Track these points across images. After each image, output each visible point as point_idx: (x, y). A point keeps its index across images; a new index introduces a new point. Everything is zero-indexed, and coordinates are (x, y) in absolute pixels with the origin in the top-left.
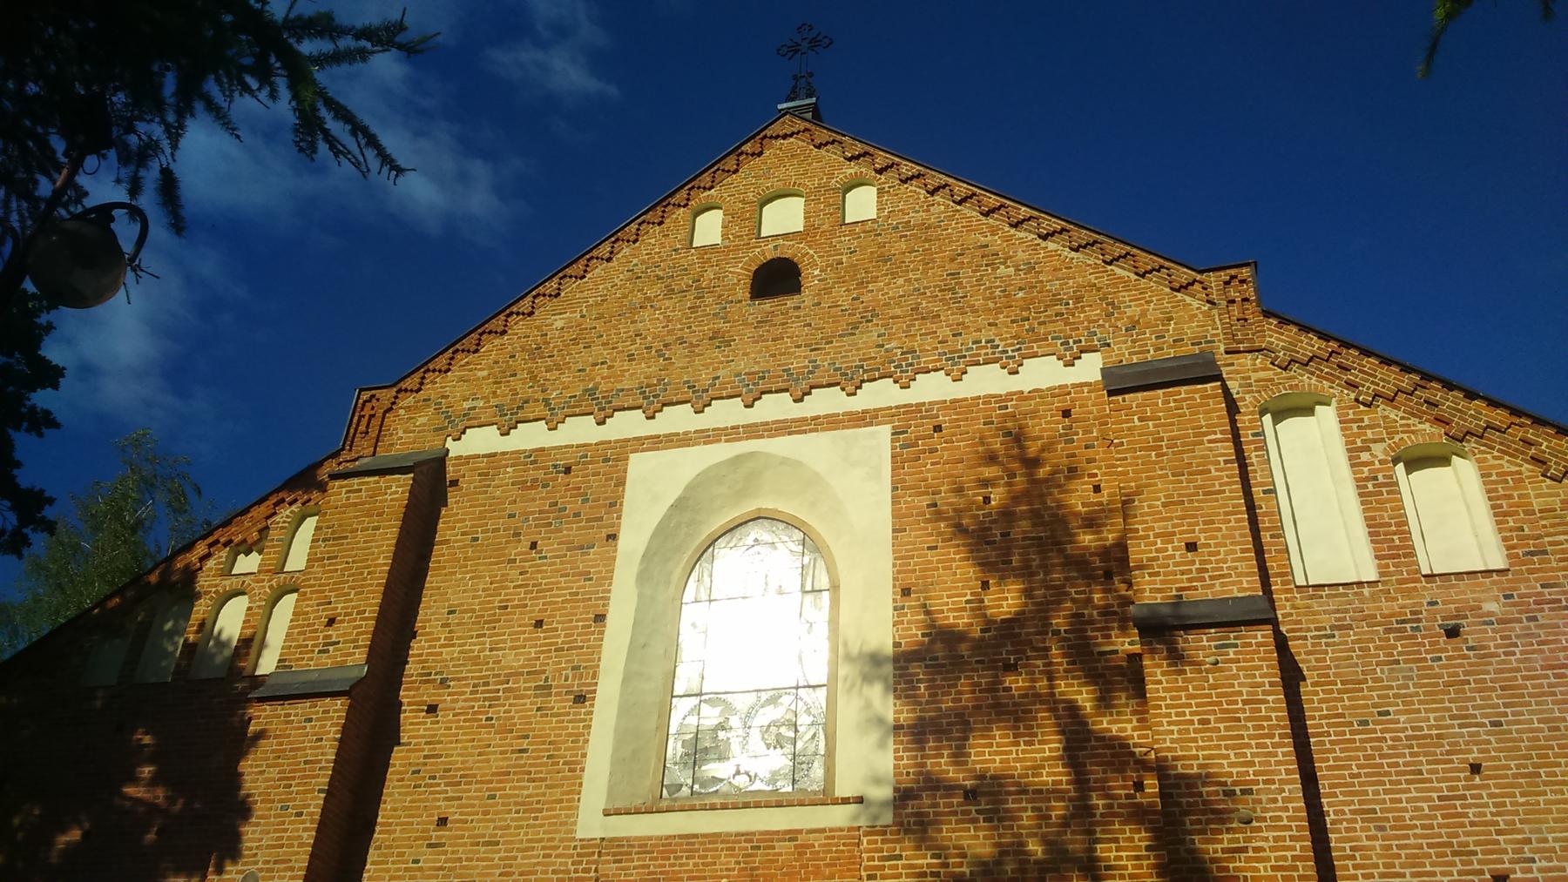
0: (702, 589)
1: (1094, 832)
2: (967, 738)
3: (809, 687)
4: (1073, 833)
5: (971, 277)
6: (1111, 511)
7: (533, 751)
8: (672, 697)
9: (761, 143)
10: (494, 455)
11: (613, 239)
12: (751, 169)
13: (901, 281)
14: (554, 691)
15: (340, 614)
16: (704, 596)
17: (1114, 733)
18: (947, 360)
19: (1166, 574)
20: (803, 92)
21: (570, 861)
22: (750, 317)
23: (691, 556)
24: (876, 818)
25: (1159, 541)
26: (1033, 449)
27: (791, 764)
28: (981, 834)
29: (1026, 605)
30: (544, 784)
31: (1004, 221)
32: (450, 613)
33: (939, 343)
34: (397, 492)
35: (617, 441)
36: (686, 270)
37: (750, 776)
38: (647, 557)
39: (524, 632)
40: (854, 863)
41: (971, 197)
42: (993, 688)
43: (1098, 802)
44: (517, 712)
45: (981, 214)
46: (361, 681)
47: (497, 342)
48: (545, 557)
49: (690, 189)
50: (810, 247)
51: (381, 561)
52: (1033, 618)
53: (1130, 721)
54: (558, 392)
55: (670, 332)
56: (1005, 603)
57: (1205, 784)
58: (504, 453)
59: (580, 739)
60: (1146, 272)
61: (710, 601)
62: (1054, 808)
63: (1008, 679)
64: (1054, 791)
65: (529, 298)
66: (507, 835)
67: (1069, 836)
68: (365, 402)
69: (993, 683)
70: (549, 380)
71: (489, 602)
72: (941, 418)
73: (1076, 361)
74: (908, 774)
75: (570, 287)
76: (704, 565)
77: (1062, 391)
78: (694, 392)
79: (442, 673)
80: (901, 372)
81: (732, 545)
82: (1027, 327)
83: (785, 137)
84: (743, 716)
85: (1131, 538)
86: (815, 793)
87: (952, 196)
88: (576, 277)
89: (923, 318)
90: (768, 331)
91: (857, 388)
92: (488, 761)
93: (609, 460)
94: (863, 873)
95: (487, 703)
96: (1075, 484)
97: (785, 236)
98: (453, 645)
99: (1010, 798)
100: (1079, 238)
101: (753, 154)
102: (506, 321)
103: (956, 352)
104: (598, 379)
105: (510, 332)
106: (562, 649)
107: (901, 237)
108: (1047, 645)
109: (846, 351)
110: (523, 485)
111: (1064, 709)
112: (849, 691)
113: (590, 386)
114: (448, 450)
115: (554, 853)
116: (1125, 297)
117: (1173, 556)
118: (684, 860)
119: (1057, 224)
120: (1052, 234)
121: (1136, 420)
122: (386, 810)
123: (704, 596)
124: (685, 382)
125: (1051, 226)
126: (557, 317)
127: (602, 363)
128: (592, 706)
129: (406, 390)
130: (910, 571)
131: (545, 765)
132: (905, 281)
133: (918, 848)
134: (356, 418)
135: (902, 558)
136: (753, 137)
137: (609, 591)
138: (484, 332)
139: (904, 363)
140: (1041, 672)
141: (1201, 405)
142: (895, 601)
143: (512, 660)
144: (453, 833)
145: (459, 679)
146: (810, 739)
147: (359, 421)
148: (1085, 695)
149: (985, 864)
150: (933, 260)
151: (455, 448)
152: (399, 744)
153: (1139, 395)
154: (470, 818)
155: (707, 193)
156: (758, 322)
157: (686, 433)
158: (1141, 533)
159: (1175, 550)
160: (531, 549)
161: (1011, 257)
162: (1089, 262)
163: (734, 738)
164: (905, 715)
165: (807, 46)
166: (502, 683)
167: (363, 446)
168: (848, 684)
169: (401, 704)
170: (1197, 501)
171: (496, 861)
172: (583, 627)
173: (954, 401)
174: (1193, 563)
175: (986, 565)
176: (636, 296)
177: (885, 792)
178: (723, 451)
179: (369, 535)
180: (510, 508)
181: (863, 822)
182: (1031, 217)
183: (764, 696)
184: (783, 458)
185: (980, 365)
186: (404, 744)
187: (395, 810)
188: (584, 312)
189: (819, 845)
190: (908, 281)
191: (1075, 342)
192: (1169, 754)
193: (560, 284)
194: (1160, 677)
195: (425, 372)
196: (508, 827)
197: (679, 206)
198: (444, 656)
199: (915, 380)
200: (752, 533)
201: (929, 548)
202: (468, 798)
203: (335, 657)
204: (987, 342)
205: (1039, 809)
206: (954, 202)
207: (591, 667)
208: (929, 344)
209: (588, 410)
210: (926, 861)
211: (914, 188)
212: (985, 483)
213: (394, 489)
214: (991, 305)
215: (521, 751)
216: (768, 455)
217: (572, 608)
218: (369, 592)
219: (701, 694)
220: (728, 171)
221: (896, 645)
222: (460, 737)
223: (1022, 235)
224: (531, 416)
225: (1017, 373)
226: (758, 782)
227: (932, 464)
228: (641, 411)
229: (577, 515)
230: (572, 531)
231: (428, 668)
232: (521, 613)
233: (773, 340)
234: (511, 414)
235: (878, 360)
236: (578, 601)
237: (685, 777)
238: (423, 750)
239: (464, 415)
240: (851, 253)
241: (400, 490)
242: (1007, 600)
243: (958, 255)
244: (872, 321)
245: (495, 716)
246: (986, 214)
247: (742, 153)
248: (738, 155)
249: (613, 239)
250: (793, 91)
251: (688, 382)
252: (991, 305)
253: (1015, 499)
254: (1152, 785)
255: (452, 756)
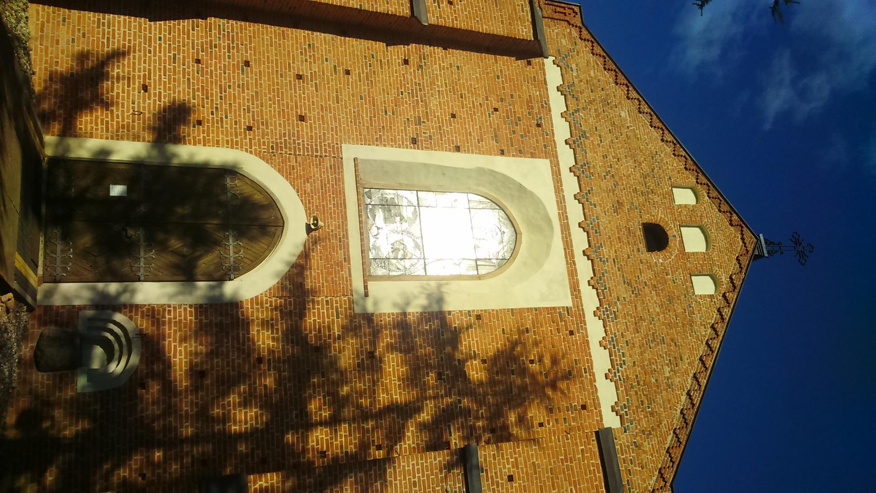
0: (476, 204)
1: (354, 423)
2: (401, 352)
3: (425, 265)
4: (353, 411)
5: (662, 351)
6: (529, 432)
7: (386, 118)
8: (417, 191)
9: (738, 225)
10: (546, 83)
11: (675, 142)
12: (722, 220)
13: (658, 310)
14: (418, 127)
15: (455, 7)
16: (472, 205)
17: (407, 434)
18: (612, 338)
19: (495, 464)
20: (770, 248)
21: (330, 142)
22: (632, 224)
23: (493, 197)
24: (357, 304)
25: (513, 460)
26: (563, 385)
27: (384, 257)
28: (351, 361)
29: (474, 384)
30: (369, 125)
31: (697, 370)
32: (458, 67)
33: (622, 333)
34: (523, 32)
35: (556, 151)
36: (659, 185)
37: (377, 235)
38: (493, 173)
39: (449, 108)
40: (334, 293)
41: (711, 350)
42: (429, 366)
43: (370, 424)
44: (406, 107)
45: (701, 356)
46: (419, 22)
47: (611, 80)
48: (490, 117)
49: (707, 184)
50: (676, 256)
51: (484, 27)
52: (467, 389)
53: (413, 443)
54: (583, 117)
55: (621, 178)
56: (475, 373)
57: (381, 484)
58: (547, 89)
59: (394, 142)
60: (670, 454)
61: (469, 209)
62: (366, 400)
63: (433, 375)
64: (375, 401)
65: (637, 96)
66: (342, 107)
67: (352, 409)
68: (573, 9)
69: (431, 366)
70: (590, 111)
71: (464, 87)
72: (578, 335)
73: (615, 413)
74: (381, 321)
75: (645, 119)
76: (489, 204)
77: (597, 405)
78: (586, 193)
79: (425, 65)
80: (604, 311)
81: (501, 219)
82: (634, 384)
83: (743, 239)
84: (408, 230)
85: (514, 444)
86: (370, 271)
87: (711, 339)
88: (651, 122)
89: (636, 323)
90: (624, 234)
91: (593, 286)
92: (380, 94)
93: (545, 148)
94: (329, 298)
95: (410, 91)
96: (543, 411)
97: (682, 242)
98: (440, 71)
99: (370, 377)
100: (689, 414)
101: (731, 220)
102: (623, 84)
103: (617, 343)
104: (592, 139)
105: (617, 87)
106: (440, 130)
107: (685, 310)
108: (453, 396)
109: (614, 279)
110: (529, 102)
111: (419, 406)
112: (423, 287)
113: (587, 135)
114: (547, 58)
115: (334, 133)
116: (655, 441)
117: (505, 467)
118: (332, 202)
119: (697, 401)
120: (690, 398)
121: (582, 447)
122: (352, 42)
123: (472, 205)
124: (592, 188)
125: (695, 398)
126: (627, 113)
127: (601, 140)
128: (411, 148)
129: (581, 32)
130: (490, 318)
131: (379, 125)
132: (658, 313)
133: (343, 327)
134: (563, 5)
135: (497, 314)
136: (741, 220)
137: (472, 153)
138: (616, 72)
139: (608, 313)
140: (437, 393)
141: (592, 485)
142: (474, 311)
143: (433, 103)
144: (342, 79)
145: (422, 75)
146: (398, 267)
147: (562, 7)
148: (426, 417)
149: (336, 363)
150: (671, 328)
151: (548, 62)
152: (387, 46)
153: (597, 449)
154: (350, 87)
155: (706, 194)
156: (629, 228)
157: (562, 190)
158: (517, 450)
159: (509, 469)
160: (494, 109)
161: (675, 374)
162: (674, 420)
163: (397, 225)
164: (412, 318)
165: (800, 250)
166: (421, 98)
167: (548, 10)
168: (427, 287)
169: (408, 45)
170: (537, 482)
171: (328, 103)
172: (453, 140)
173: (588, 342)
174: (502, 479)
175: (495, 359)
176: (641, 157)
177: (370, 308)
178: (553, 211)
179: (498, 19)
180: (516, 95)
181: (355, 296)
182: (700, 386)
183: (419, 241)
184: (551, 246)
185: (610, 357)
186: (387, 49)
187: (353, 46)
188: (630, 128)
189: (343, 274)
190: (658, 314)
191: (626, 412)
192: (397, 465)
193: (647, 113)
194: (438, 459)
195: (591, 41)
196: (346, 108)
197: (697, 179)
198: (435, 66)
199: (599, 319)
200: (508, 230)
201: (503, 329)
202: (360, 85)
203: (432, 7)
204: (624, 361)
205: (365, 393)
206: (708, 340)
207: (431, 146)
208: (620, 327)
209: (574, 135)
210: (336, 331)
211: (715, 316)
212: (541, 360)
213: (524, 30)
214: (646, 363)
215: (386, 112)
216: (552, 237)
217: (463, 133)
218: (467, 22)
219: (419, 206)
220: (720, 207)
221: (450, 312)
222: (392, 78)
223: (690, 381)
224: (569, 103)
225: (606, 379)
226: (374, 239)
227: (551, 330)
228: (574, 164)
229: (514, 132)
230: (505, 131)
231: (428, 58)
232: (459, 106)
233: (619, 237)
234: (569, 91)
235: (610, 298)
236: (467, 136)
237: (375, 200)
238: (384, 59)
239: (568, 65)
240: (673, 280)
241: (524, 34)
242: (476, 372)
243: (675, 344)
244: (633, 294)
245: (404, 96)
246: (701, 359)
247: (731, 214)
248: (730, 212)
249: (675, 142)
250: (771, 243)
251: (592, 190)
252: (646, 363)
253: (533, 376)
254: (380, 454)
255: (382, 75)
